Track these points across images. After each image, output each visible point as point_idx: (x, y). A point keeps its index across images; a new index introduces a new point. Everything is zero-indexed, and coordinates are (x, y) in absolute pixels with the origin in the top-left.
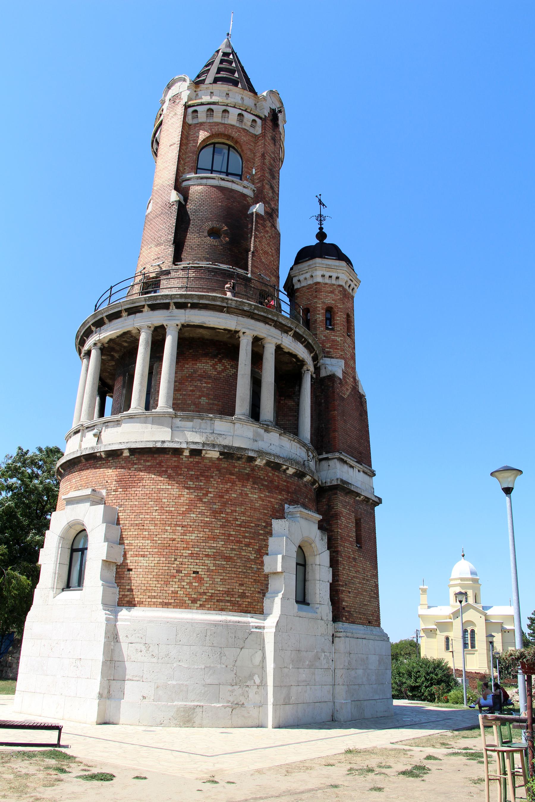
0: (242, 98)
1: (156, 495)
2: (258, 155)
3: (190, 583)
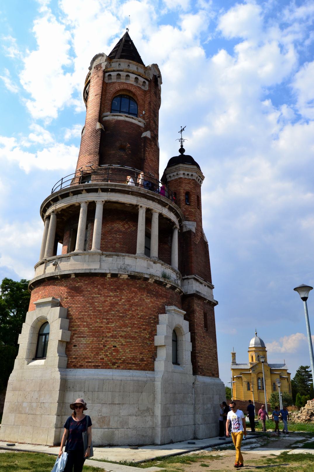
0: (137, 68)
2: (147, 102)
3: (111, 354)
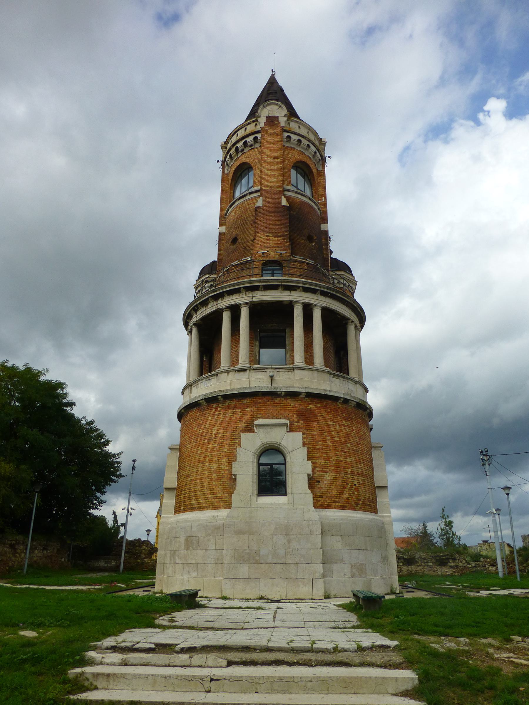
1: (327, 428)
